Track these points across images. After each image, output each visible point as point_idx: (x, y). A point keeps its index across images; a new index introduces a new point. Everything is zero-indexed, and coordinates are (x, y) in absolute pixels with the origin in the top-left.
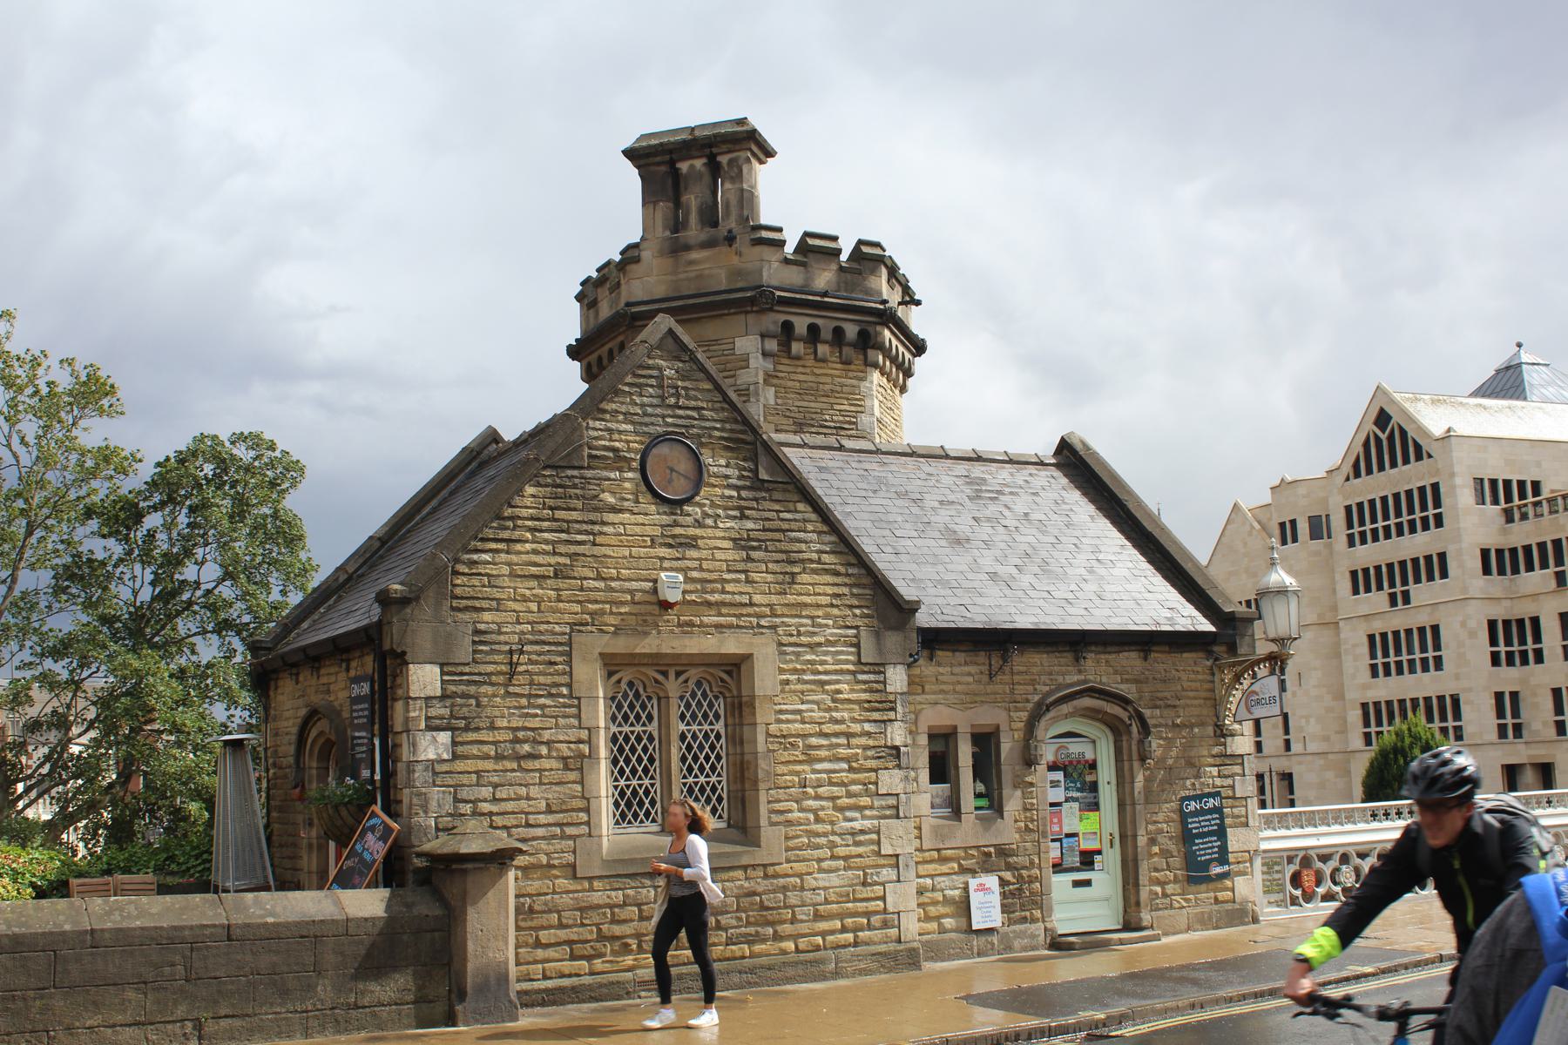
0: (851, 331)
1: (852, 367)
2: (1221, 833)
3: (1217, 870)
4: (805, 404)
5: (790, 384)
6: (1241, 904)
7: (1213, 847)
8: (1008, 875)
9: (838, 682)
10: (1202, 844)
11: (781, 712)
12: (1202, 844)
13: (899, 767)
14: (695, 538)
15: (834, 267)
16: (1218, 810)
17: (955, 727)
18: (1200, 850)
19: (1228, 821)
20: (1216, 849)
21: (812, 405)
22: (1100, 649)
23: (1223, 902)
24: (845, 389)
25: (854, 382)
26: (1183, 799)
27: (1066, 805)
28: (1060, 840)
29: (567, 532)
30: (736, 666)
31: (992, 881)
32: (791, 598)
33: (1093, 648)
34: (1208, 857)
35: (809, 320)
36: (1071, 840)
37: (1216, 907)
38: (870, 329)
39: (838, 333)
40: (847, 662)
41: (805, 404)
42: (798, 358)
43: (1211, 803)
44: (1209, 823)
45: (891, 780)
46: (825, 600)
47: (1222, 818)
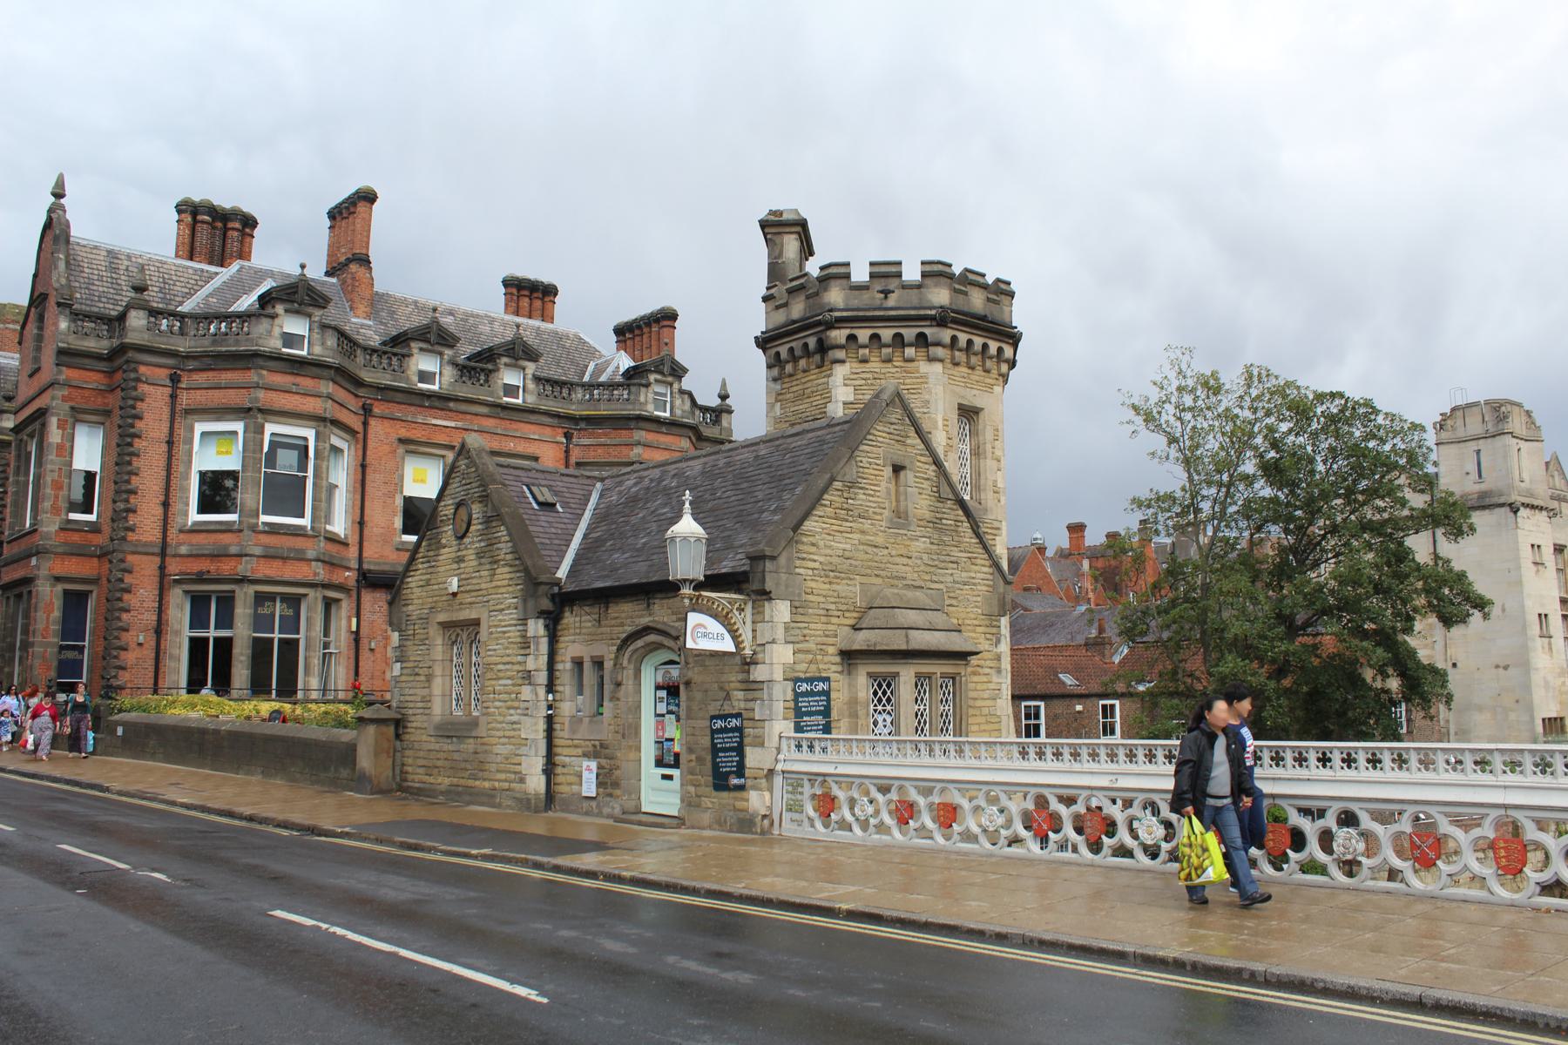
0: (812, 342)
1: (824, 368)
2: (740, 750)
3: (735, 781)
4: (796, 408)
5: (788, 396)
6: (752, 815)
7: (732, 761)
8: (603, 762)
9: (509, 631)
10: (725, 757)
11: (489, 650)
12: (725, 757)
13: (530, 684)
14: (464, 556)
15: (802, 297)
16: (740, 730)
17: (582, 657)
18: (722, 762)
19: (746, 740)
20: (735, 764)
21: (801, 407)
22: (663, 595)
23: (739, 810)
24: (820, 388)
25: (825, 380)
26: (713, 717)
27: (667, 716)
28: (662, 742)
29: (429, 562)
30: (476, 623)
31: (593, 765)
32: (494, 584)
33: (659, 596)
34: (728, 769)
35: (788, 346)
36: (669, 743)
37: (731, 813)
38: (823, 336)
40: (512, 619)
41: (796, 408)
42: (791, 375)
43: (734, 722)
44: (730, 740)
45: (526, 692)
46: (506, 582)
47: (742, 737)
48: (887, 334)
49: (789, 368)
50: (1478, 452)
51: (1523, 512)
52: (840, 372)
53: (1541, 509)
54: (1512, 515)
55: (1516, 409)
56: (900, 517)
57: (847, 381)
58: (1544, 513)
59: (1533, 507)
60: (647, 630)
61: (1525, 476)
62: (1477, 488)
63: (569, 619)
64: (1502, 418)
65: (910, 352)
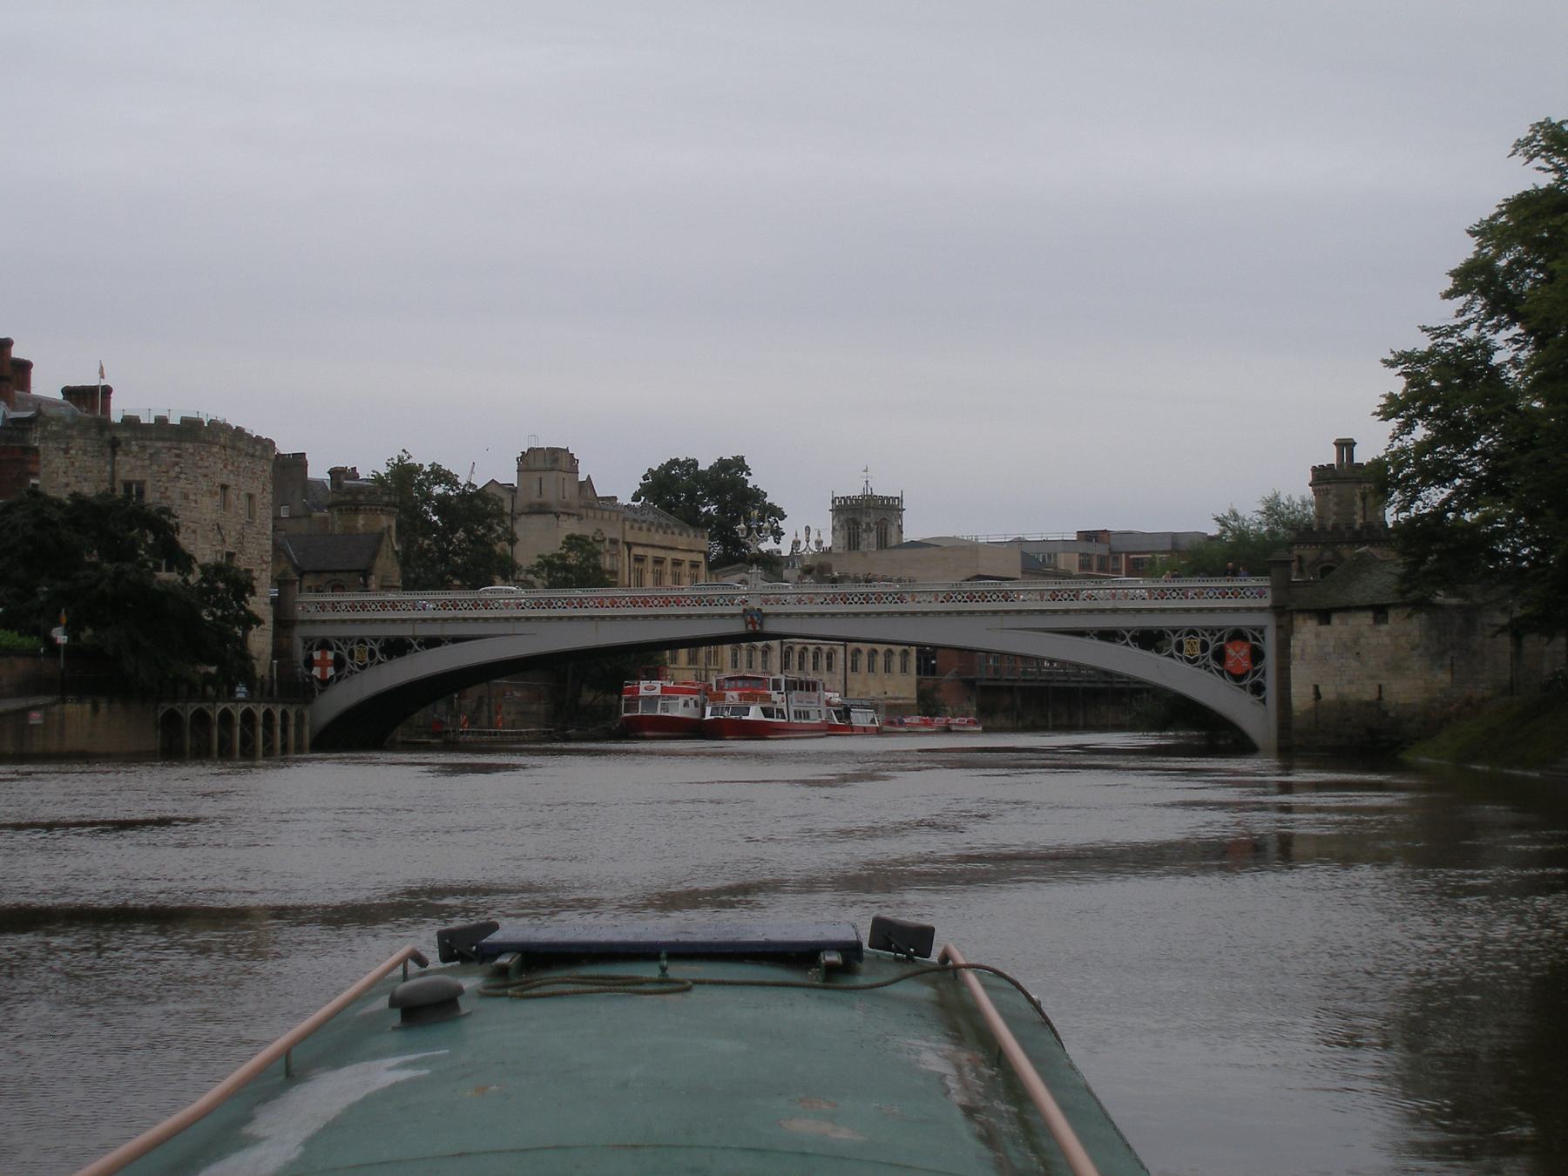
0: (353, 508)
39: (351, 509)
48: (373, 507)
49: (344, 512)
50: (541, 479)
51: (562, 517)
52: (361, 517)
53: (573, 515)
54: (555, 519)
55: (564, 453)
56: (387, 557)
57: (363, 519)
58: (576, 517)
59: (569, 514)
60: (335, 580)
61: (567, 495)
62: (539, 500)
63: (305, 576)
64: (556, 460)
65: (378, 512)
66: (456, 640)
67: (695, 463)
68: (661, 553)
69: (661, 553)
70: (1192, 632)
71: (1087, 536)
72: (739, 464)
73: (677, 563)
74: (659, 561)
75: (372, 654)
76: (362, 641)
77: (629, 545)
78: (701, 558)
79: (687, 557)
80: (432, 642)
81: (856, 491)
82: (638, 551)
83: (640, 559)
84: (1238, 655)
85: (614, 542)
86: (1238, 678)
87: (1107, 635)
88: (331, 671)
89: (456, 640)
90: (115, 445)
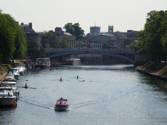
66: (58, 53)
67: (72, 23)
68: (71, 39)
69: (71, 39)
70: (128, 54)
71: (128, 31)
72: (78, 24)
73: (73, 40)
74: (70, 40)
75: (50, 54)
76: (49, 53)
77: (67, 38)
78: (75, 39)
79: (74, 39)
80: (56, 53)
81: (93, 26)
82: (68, 39)
83: (68, 40)
84: (132, 56)
85: (66, 38)
86: (132, 58)
87: (120, 54)
88: (45, 56)
89: (58, 53)
90: (29, 35)
